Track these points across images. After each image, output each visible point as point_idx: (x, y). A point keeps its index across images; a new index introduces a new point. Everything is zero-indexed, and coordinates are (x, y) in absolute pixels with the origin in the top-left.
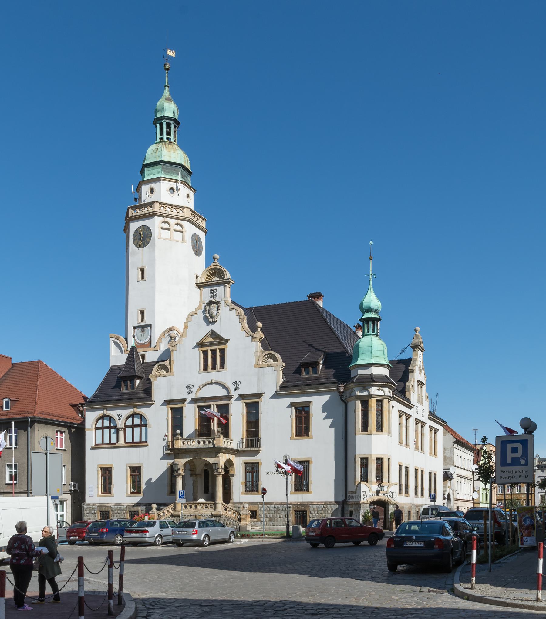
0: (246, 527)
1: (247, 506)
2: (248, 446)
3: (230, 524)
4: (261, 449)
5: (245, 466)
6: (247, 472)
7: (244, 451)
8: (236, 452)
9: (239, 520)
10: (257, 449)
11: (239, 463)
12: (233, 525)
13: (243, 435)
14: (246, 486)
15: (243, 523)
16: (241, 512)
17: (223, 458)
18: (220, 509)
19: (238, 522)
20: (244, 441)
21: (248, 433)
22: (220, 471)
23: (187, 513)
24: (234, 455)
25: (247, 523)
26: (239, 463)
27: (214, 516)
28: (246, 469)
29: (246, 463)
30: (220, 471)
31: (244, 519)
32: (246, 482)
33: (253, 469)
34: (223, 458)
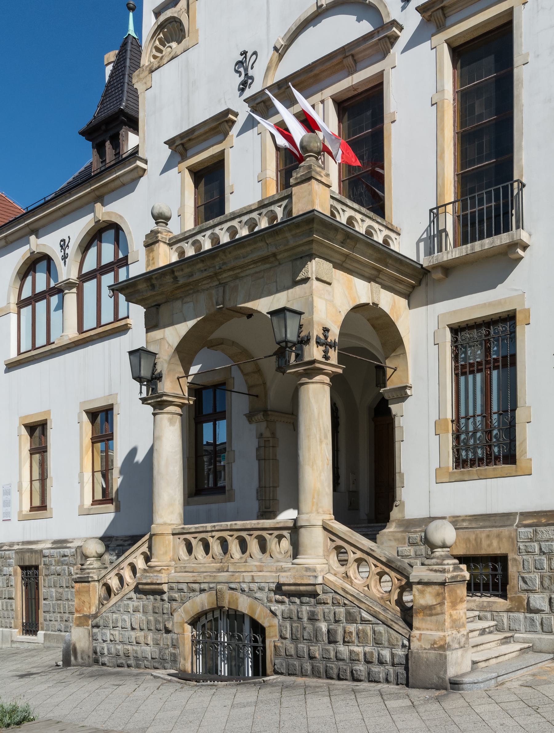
0: (442, 662)
1: (445, 533)
2: (466, 236)
3: (361, 637)
4: (524, 236)
5: (455, 341)
6: (461, 370)
7: (447, 269)
8: (416, 281)
9: (407, 615)
10: (503, 239)
11: (423, 334)
12: (377, 643)
13: (439, 195)
14: (457, 437)
15: (424, 633)
16: (418, 573)
17: (330, 297)
18: (318, 561)
19: (400, 626)
20: (449, 222)
21: (467, 183)
22: (315, 352)
23: (189, 577)
24: (407, 296)
25: (450, 635)
26: (423, 334)
27: (289, 595)
28: (456, 358)
29: (456, 330)
30: (315, 352)
31: (429, 610)
32: (457, 421)
33: (488, 351)
34: (330, 297)
